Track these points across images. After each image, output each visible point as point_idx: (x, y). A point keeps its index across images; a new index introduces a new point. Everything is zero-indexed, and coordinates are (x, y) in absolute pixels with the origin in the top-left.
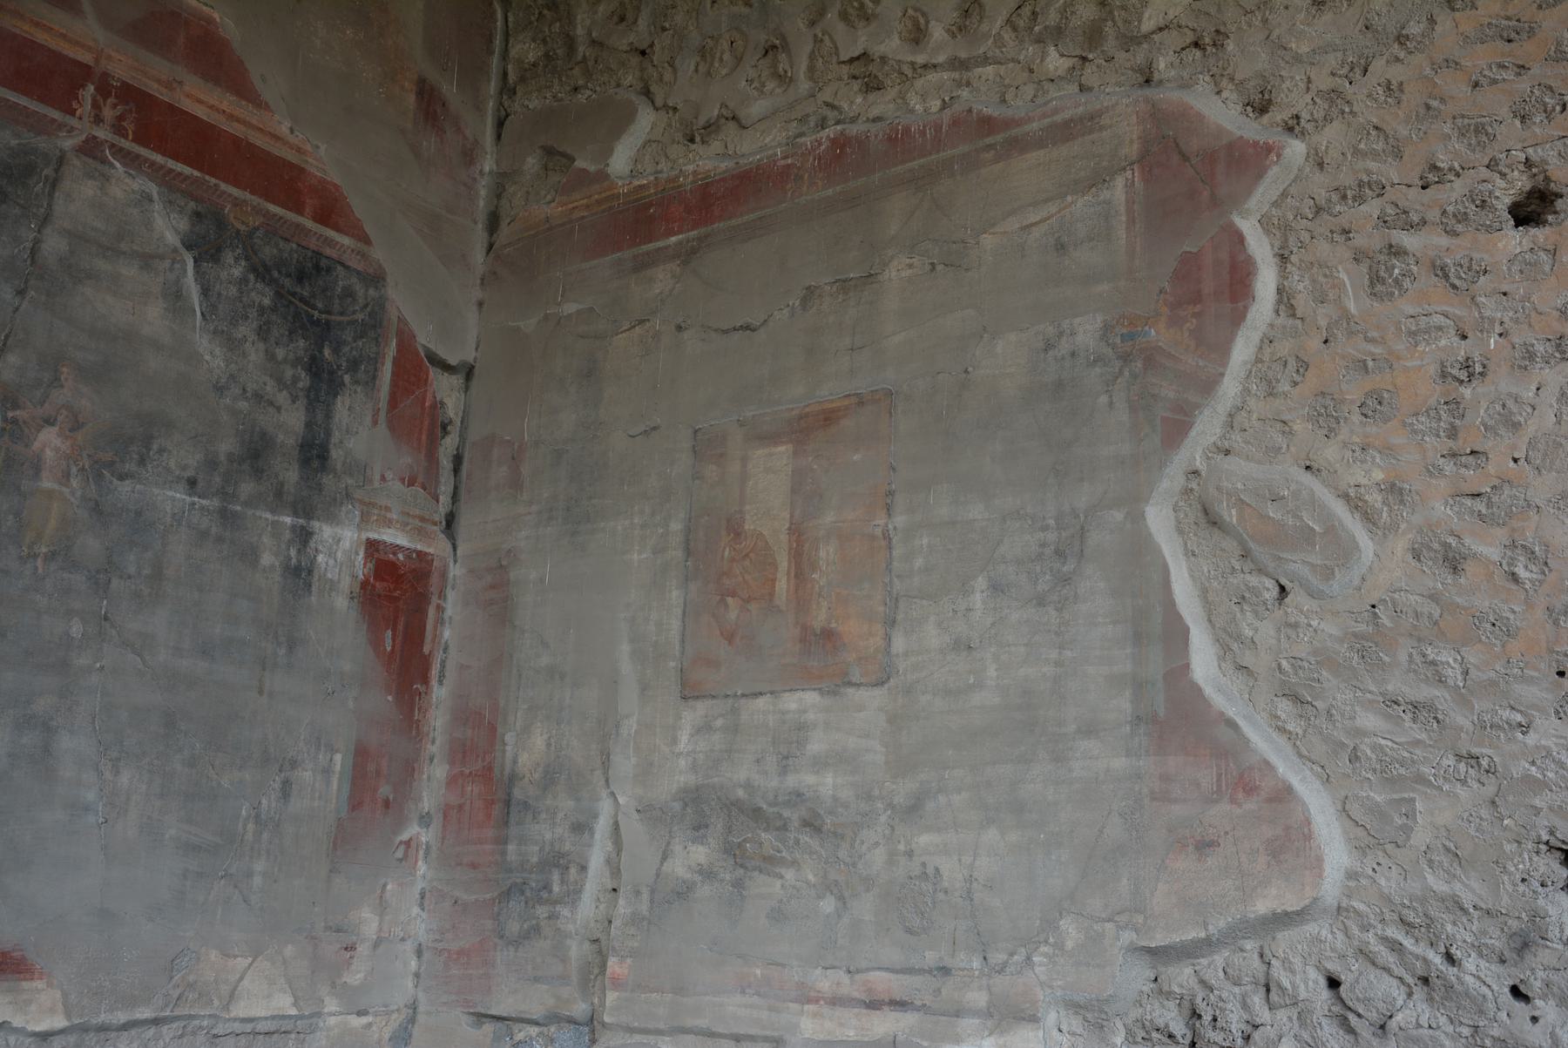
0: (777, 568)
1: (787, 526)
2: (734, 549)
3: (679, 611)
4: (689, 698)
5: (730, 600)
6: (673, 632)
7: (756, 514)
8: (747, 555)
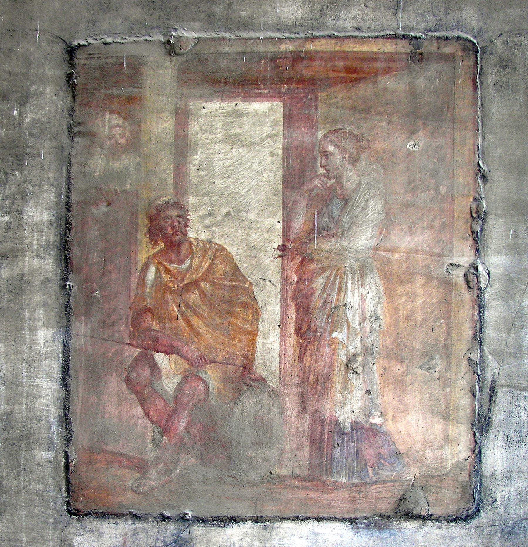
0: (257, 313)
1: (278, 242)
2: (167, 270)
3: (55, 367)
4: (86, 515)
5: (160, 358)
6: (44, 401)
7: (210, 214)
8: (195, 284)
